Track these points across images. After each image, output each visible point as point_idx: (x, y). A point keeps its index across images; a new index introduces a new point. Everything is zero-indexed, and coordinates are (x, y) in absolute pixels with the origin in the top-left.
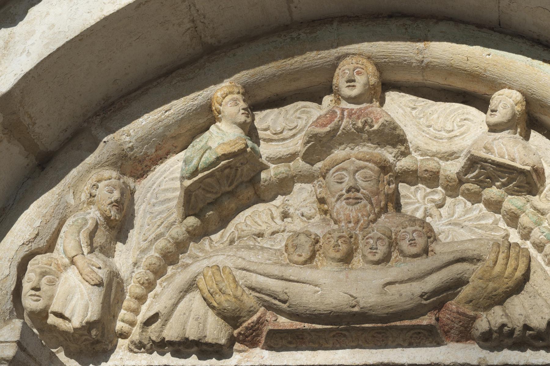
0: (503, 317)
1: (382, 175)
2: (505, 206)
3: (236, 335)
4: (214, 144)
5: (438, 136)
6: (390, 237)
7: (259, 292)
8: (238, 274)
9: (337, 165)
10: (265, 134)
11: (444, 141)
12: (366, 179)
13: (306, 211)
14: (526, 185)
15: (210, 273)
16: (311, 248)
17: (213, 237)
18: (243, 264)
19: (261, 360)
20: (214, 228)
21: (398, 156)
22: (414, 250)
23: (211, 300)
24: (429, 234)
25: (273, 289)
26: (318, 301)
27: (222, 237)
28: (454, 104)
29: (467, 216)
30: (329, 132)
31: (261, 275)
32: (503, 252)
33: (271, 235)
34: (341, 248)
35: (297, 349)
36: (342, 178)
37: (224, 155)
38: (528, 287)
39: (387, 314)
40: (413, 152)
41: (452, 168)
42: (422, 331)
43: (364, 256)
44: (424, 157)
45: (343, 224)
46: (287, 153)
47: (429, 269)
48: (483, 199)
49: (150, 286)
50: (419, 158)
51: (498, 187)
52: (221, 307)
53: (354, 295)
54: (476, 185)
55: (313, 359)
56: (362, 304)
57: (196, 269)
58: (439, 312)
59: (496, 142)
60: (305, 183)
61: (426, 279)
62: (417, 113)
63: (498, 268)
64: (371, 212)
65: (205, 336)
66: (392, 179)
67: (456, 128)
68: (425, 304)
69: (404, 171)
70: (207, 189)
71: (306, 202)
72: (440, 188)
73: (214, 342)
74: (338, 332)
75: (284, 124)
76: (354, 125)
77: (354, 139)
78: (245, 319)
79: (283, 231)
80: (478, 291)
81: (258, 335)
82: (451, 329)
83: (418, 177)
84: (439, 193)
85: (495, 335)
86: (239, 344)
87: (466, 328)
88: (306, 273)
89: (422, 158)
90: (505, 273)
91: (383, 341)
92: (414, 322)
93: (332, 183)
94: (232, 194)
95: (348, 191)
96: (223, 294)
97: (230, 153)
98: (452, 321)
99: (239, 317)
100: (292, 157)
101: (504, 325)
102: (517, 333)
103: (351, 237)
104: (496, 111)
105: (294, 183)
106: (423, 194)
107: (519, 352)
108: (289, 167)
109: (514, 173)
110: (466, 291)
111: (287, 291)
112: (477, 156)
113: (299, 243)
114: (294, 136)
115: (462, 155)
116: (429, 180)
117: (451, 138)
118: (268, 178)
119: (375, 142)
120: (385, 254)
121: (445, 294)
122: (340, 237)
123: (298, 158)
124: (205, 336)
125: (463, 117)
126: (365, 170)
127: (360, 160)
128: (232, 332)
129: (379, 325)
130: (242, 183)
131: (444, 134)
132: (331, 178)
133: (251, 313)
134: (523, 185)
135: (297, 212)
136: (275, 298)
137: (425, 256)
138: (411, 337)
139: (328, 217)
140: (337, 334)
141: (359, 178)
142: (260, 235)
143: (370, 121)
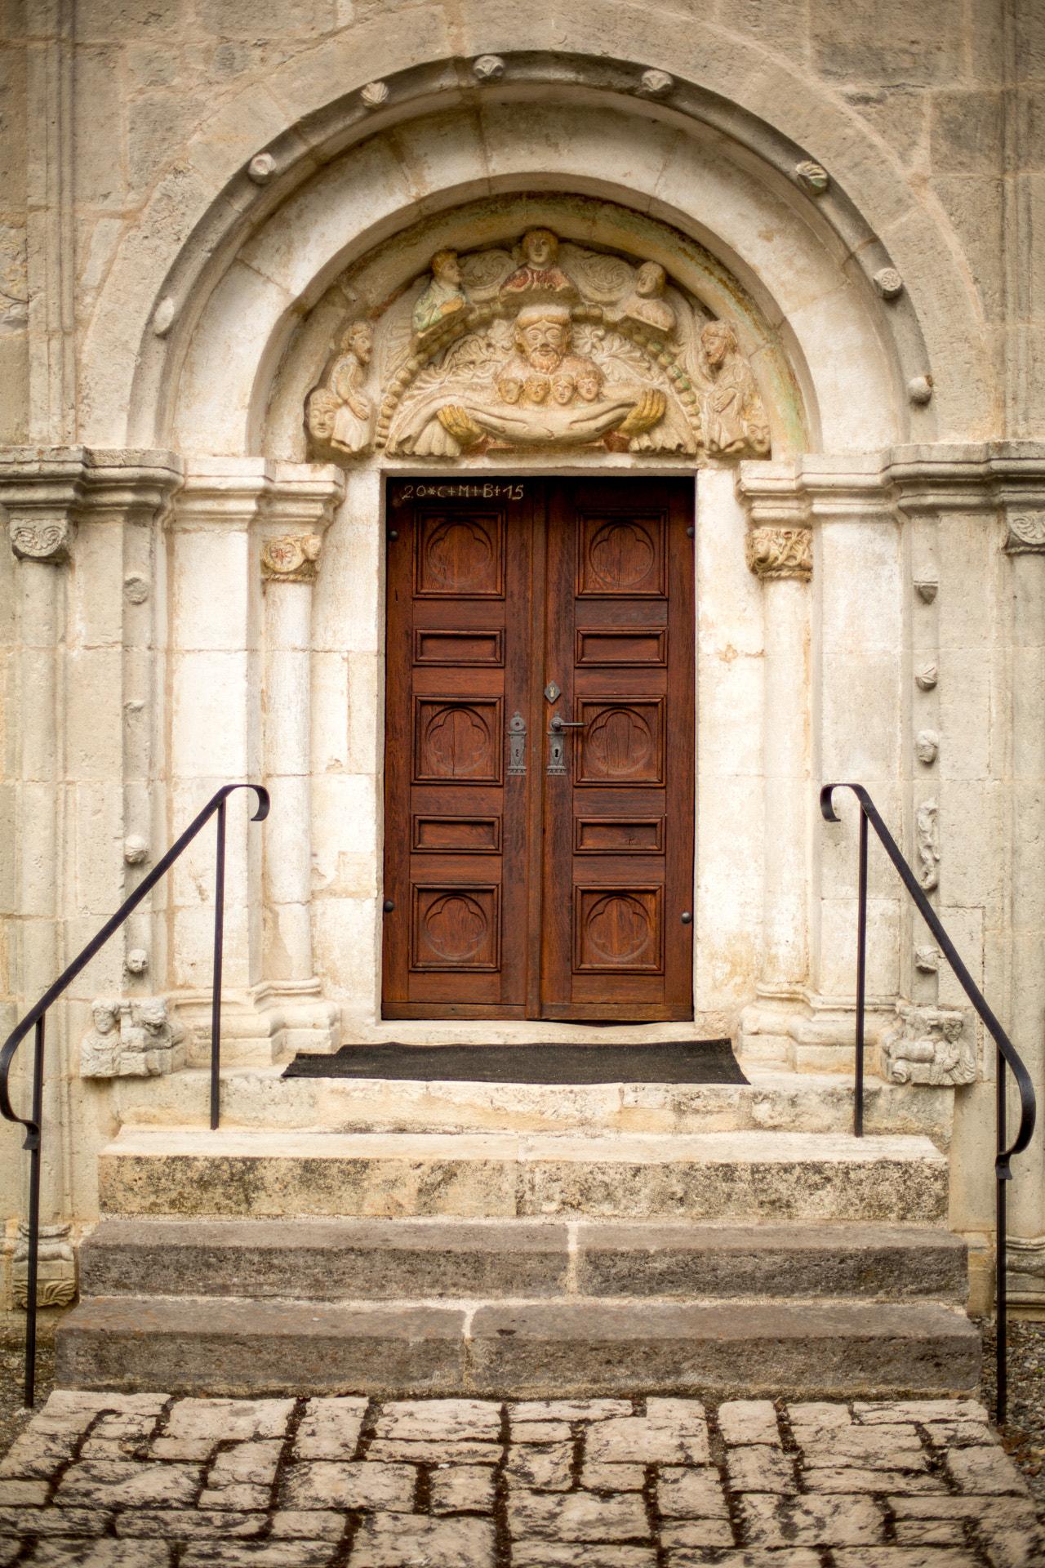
18: (472, 405)
22: (590, 397)
49: (393, 407)
133: (477, 437)
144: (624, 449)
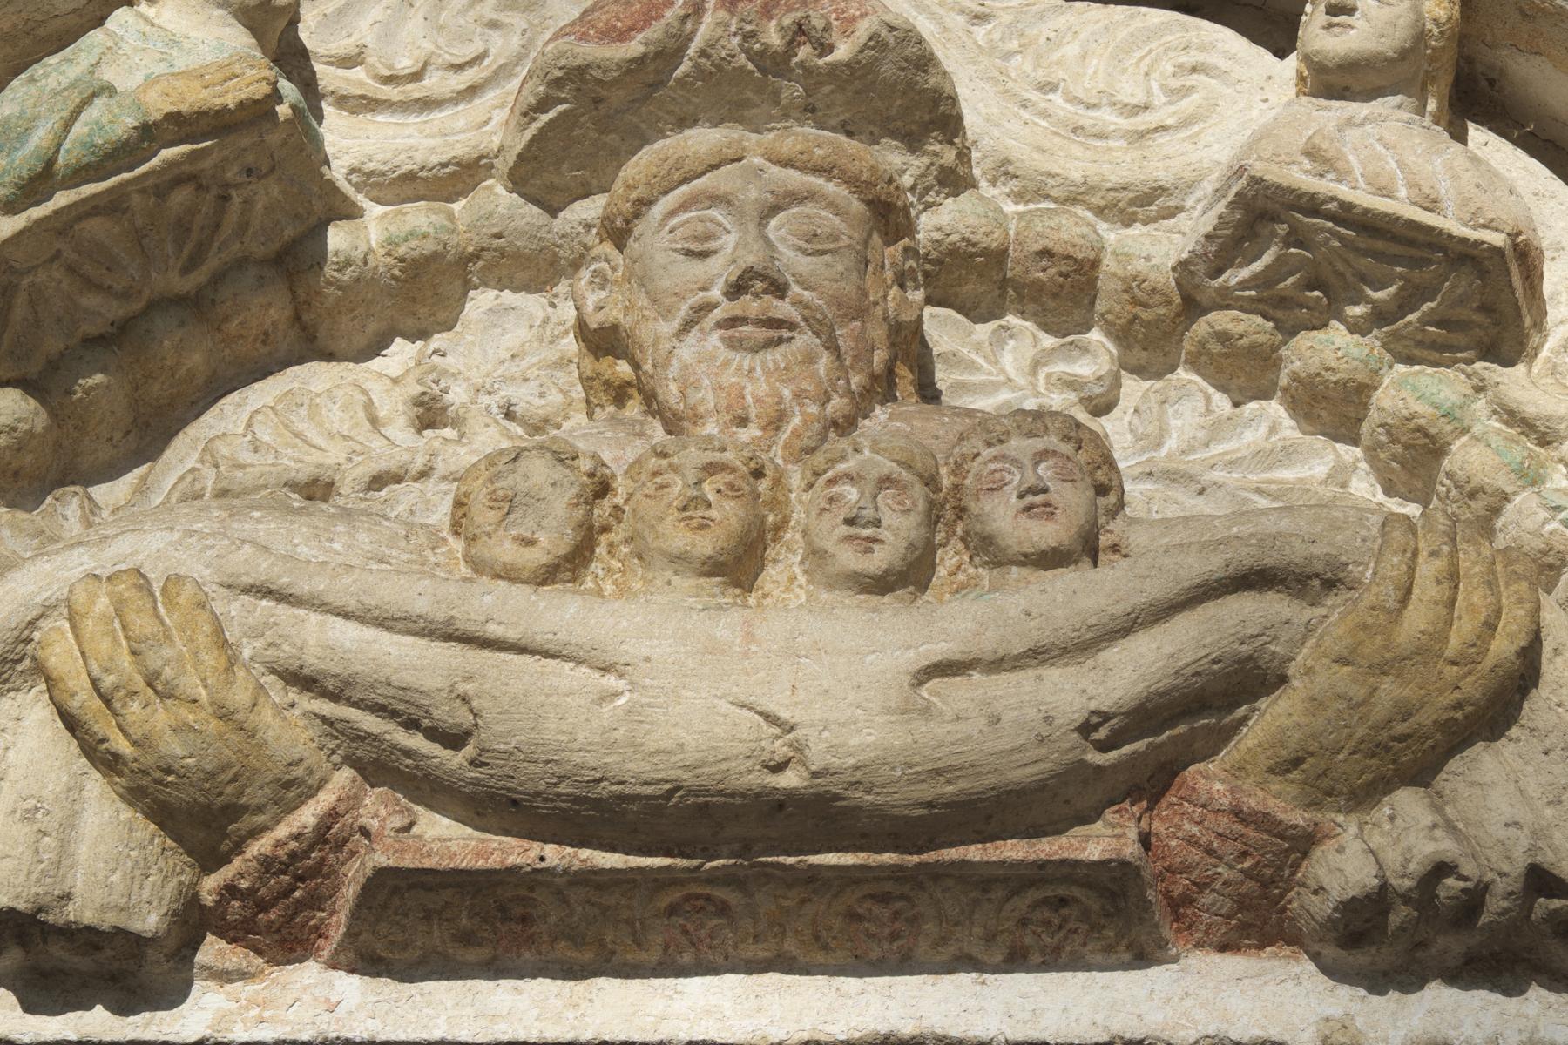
0: (1438, 833)
1: (876, 239)
2: (1387, 404)
3: (208, 899)
4: (126, 76)
5: (1087, 123)
6: (931, 481)
7: (334, 697)
8: (237, 611)
9: (686, 180)
10: (347, 80)
11: (1111, 143)
12: (812, 242)
13: (525, 398)
14: (1477, 317)
15: (103, 604)
16: (579, 513)
17: (99, 492)
18: (264, 570)
19: (326, 1017)
20: (105, 453)
21: (927, 190)
22: (1045, 534)
23: (103, 725)
24: (1101, 476)
25: (408, 678)
26: (619, 734)
27: (142, 488)
28: (1144, 9)
29: (1219, 448)
30: (641, 61)
31: (346, 615)
32: (1433, 554)
33: (369, 488)
34: (713, 513)
35: (494, 969)
36: (708, 237)
37: (174, 118)
38: (1540, 707)
39: (930, 805)
40: (983, 184)
41: (1155, 250)
42: (1076, 892)
43: (816, 555)
44: (1032, 206)
45: (711, 428)
46: (444, 158)
47: (1119, 609)
48: (1284, 380)
50: (1010, 207)
51: (1354, 328)
52: (149, 760)
53: (785, 715)
54: (1259, 320)
55: (570, 1014)
56: (818, 756)
57: (33, 588)
58: (1150, 809)
59: (1353, 134)
60: (516, 290)
61: (1103, 656)
62: (996, 36)
63: (1417, 619)
64: (832, 382)
65: (67, 897)
66: (911, 263)
67: (1159, 98)
68: (1099, 769)
69: (953, 252)
70: (87, 268)
71: (524, 364)
72: (1095, 335)
73: (109, 920)
74: (696, 889)
75: (428, 46)
76: (749, 36)
77: (745, 104)
78: (260, 819)
79: (424, 474)
80: (1330, 714)
81: (315, 901)
82: (1202, 886)
83: (1004, 283)
84: (1096, 355)
85: (1399, 915)
86: (223, 944)
87: (1266, 884)
88: (558, 613)
89: (1021, 208)
90: (1447, 639)
91: (894, 937)
92: (1046, 848)
93: (661, 258)
94: (196, 306)
95: (736, 289)
96: (164, 696)
97: (202, 114)
98: (1210, 852)
99: (234, 811)
100: (460, 177)
101: (1442, 869)
102: (1495, 904)
103: (758, 474)
104: (1350, 11)
105: (467, 286)
106: (1030, 353)
107: (1497, 997)
108: (451, 216)
109: (1430, 262)
110: (1271, 720)
111: (468, 688)
112: (1279, 187)
113: (522, 487)
114: (472, 91)
115: (1189, 202)
116: (1055, 296)
117: (1141, 135)
118: (358, 255)
119: (833, 122)
120: (911, 547)
121: (1182, 729)
122: (711, 469)
123: (490, 182)
124: (67, 897)
125: (1187, 59)
126: (808, 208)
127: (787, 163)
128: (194, 885)
129: (888, 858)
130: (241, 263)
131: (1109, 118)
132: (657, 237)
133: (293, 789)
134: (1465, 313)
135: (485, 399)
136: (412, 724)
137: (1086, 562)
138: (1023, 922)
139: (634, 409)
140: (687, 898)
141: (784, 240)
142: (317, 489)
143: (818, 23)
144: (1258, 919)
